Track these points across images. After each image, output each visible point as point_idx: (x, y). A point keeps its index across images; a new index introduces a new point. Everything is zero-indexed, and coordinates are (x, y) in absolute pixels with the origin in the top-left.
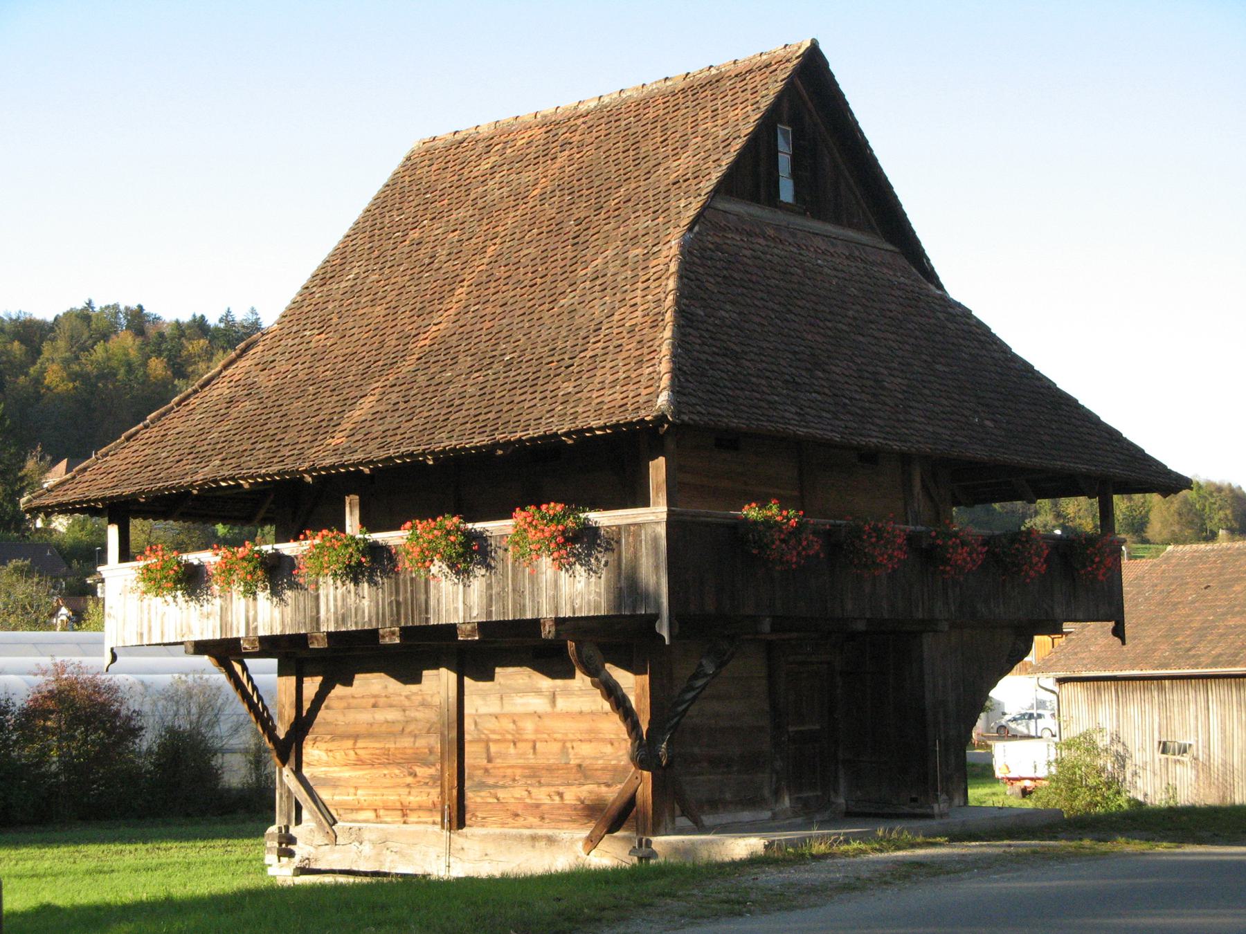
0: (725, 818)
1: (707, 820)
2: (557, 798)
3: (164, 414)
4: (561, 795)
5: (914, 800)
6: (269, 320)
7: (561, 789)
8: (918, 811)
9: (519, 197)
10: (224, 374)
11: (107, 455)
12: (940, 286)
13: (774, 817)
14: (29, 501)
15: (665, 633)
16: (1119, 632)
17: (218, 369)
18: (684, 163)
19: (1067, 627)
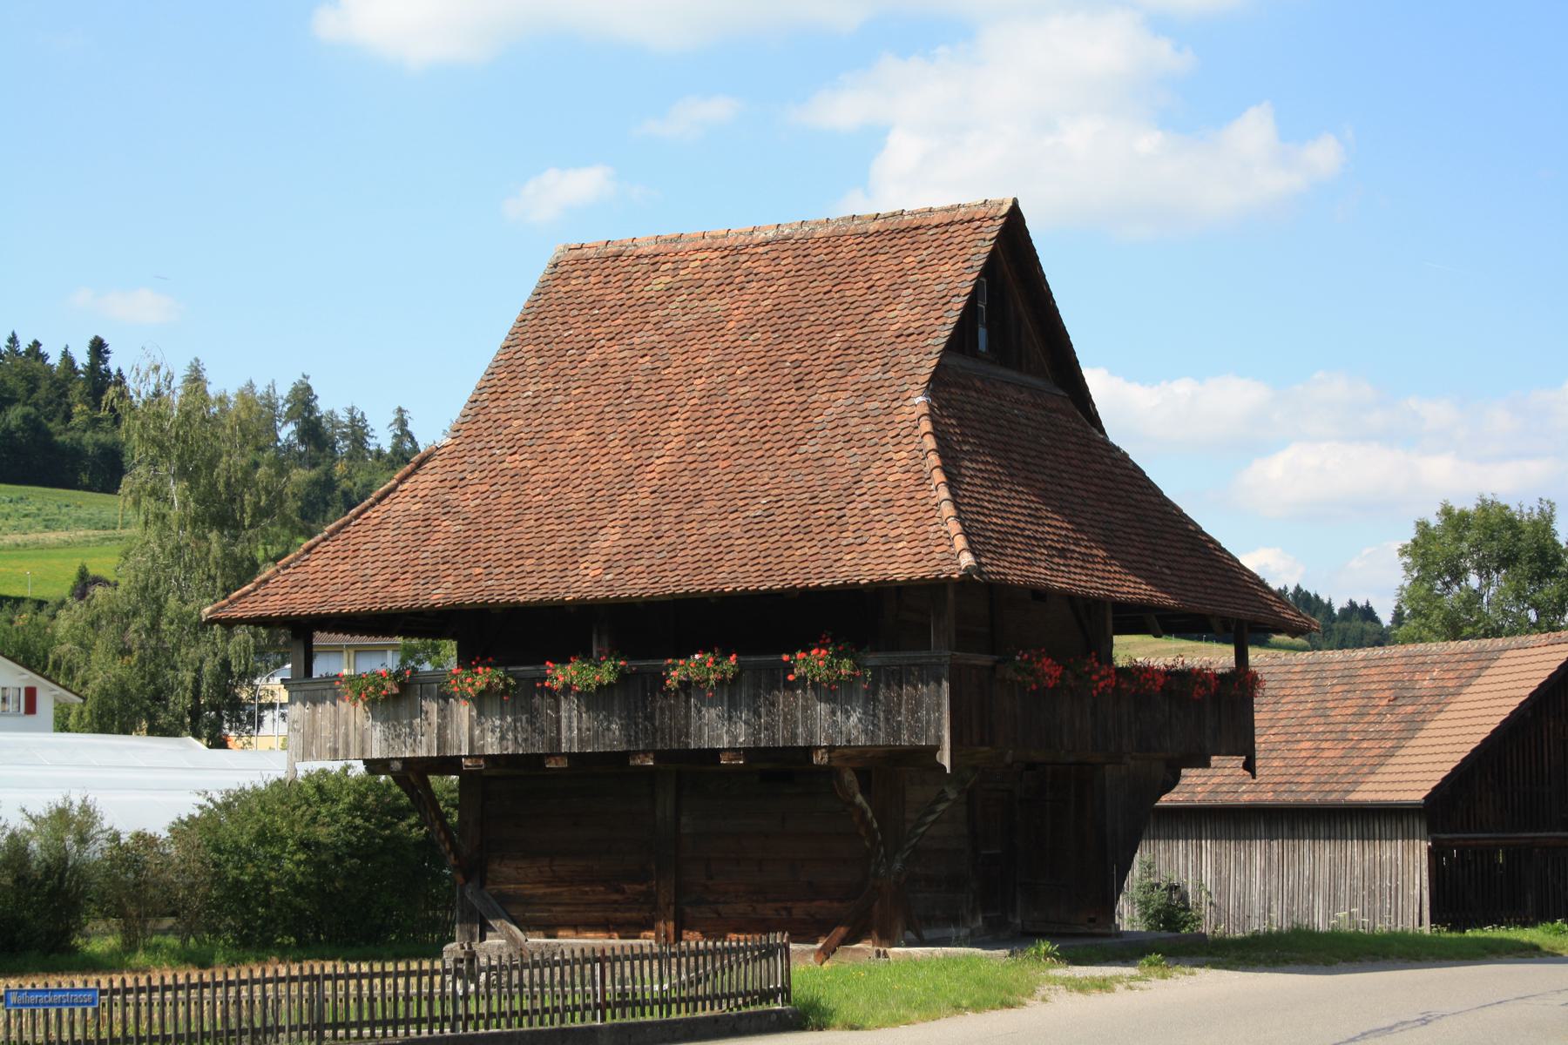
0: (935, 933)
1: (926, 934)
2: (784, 913)
3: (343, 526)
4: (789, 910)
5: (1092, 920)
6: (430, 432)
7: (789, 904)
8: (1097, 930)
9: (715, 326)
10: (400, 488)
11: (287, 567)
12: (1102, 431)
13: (972, 934)
14: (212, 612)
15: (946, 762)
16: (1250, 766)
17: (394, 482)
18: (900, 315)
19: (1215, 760)
